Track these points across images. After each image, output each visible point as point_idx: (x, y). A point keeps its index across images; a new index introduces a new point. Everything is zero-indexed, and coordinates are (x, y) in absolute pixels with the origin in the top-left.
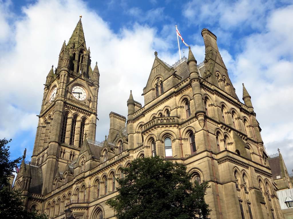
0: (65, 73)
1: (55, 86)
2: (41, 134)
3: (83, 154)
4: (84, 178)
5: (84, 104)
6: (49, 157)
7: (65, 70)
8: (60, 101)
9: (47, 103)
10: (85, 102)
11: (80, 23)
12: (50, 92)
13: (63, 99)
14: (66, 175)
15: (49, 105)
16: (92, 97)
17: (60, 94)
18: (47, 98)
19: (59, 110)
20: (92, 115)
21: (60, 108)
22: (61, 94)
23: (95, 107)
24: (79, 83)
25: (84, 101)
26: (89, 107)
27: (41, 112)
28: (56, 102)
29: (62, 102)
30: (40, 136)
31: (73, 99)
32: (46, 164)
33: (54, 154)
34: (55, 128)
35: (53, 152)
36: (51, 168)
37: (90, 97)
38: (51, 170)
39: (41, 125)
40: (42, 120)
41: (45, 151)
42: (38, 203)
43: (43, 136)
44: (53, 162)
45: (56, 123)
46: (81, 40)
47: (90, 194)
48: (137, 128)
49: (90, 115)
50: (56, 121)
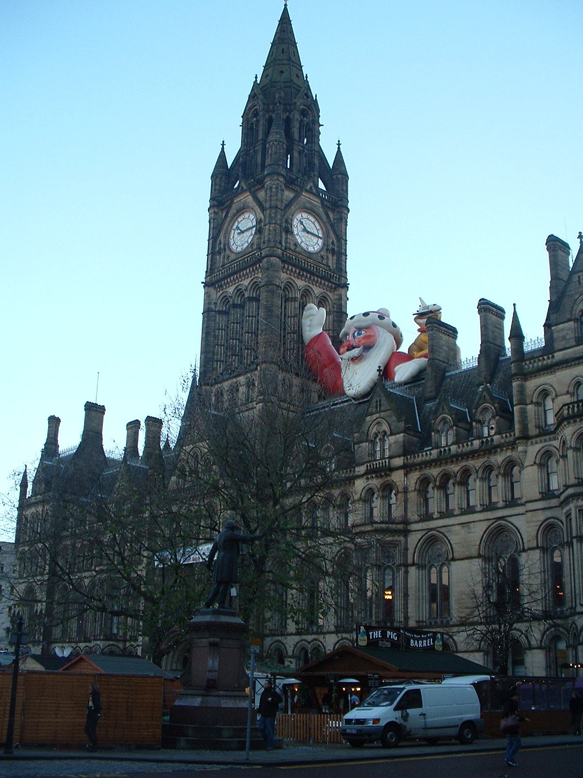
2: (214, 332)
3: (378, 415)
4: (392, 469)
11: (285, 21)
12: (230, 222)
15: (233, 257)
23: (344, 268)
25: (319, 252)
27: (210, 271)
31: (298, 249)
37: (333, 243)
39: (213, 307)
43: (222, 336)
46: (297, 75)
47: (409, 506)
48: (535, 395)
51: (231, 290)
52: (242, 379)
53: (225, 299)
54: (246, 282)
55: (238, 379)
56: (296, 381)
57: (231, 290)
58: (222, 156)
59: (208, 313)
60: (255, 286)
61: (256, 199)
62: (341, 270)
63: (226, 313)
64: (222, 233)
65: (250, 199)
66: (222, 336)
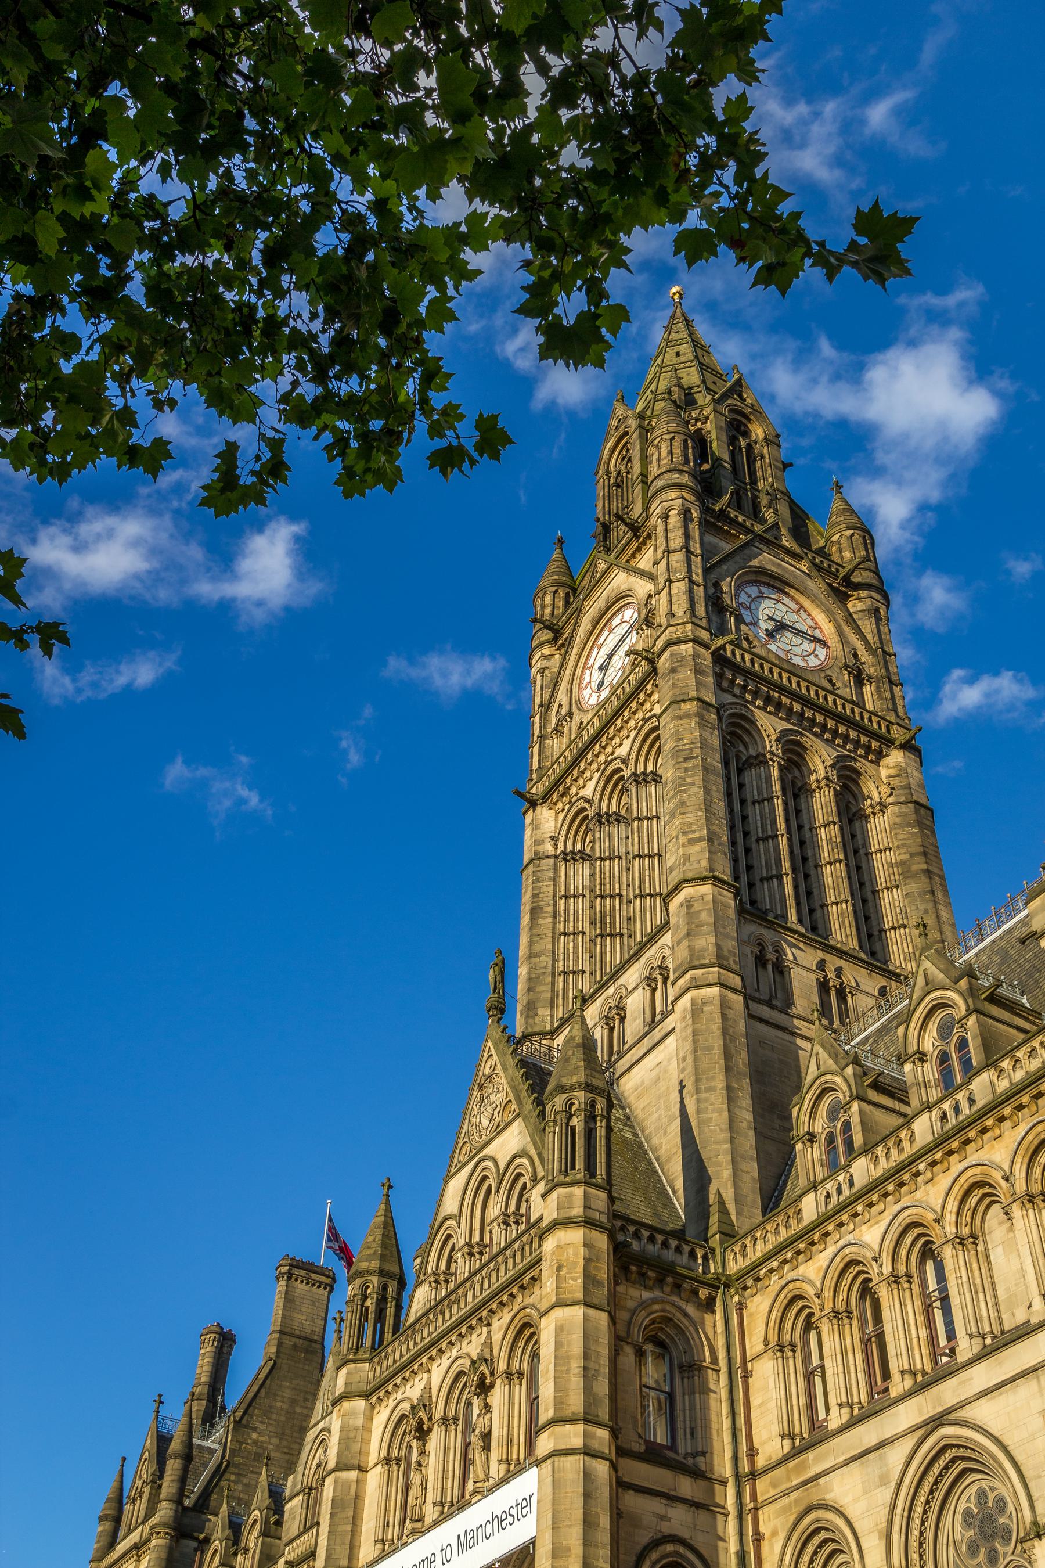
0: (683, 498)
1: (621, 598)
5: (829, 686)
6: (694, 978)
7: (680, 486)
8: (687, 648)
9: (570, 714)
10: (830, 681)
13: (705, 635)
14: (932, 1029)
16: (864, 657)
17: (681, 608)
18: (562, 697)
19: (693, 694)
20: (895, 757)
21: (699, 684)
22: (685, 605)
24: (773, 569)
26: (860, 704)
28: (659, 655)
29: (702, 651)
30: (555, 915)
32: (671, 1039)
33: (725, 963)
34: (695, 794)
35: (712, 949)
36: (728, 1056)
38: (728, 1069)
39: (548, 848)
41: (622, 981)
42: (683, 1304)
43: (576, 912)
44: (731, 1014)
45: (694, 767)
49: (880, 755)
50: (686, 759)
66: (576, 912)
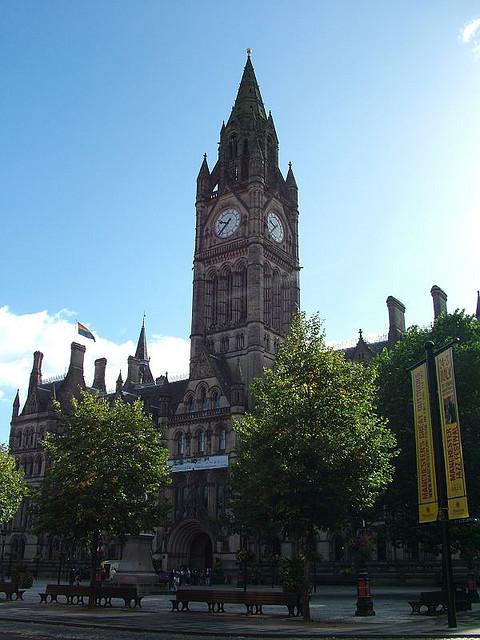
11: (249, 69)
27: (199, 250)
40: (203, 268)
51: (219, 265)
52: (232, 333)
53: (213, 273)
54: (233, 261)
55: (229, 332)
56: (272, 336)
57: (219, 265)
58: (205, 164)
59: (197, 282)
60: (241, 264)
61: (239, 199)
62: (295, 257)
63: (213, 282)
64: (209, 222)
65: (234, 199)
